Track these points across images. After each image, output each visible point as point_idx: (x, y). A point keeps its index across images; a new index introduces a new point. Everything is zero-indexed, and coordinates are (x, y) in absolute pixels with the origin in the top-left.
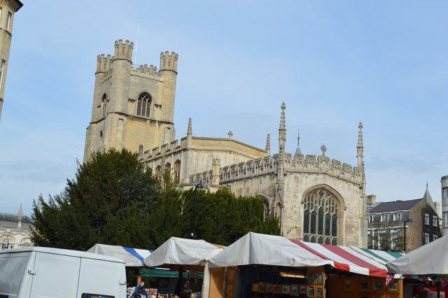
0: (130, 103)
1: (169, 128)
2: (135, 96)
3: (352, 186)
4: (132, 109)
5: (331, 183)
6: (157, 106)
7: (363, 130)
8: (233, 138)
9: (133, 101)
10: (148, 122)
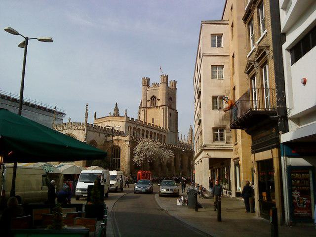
2: (149, 98)
3: (81, 131)
4: (149, 104)
6: (158, 100)
9: (149, 101)
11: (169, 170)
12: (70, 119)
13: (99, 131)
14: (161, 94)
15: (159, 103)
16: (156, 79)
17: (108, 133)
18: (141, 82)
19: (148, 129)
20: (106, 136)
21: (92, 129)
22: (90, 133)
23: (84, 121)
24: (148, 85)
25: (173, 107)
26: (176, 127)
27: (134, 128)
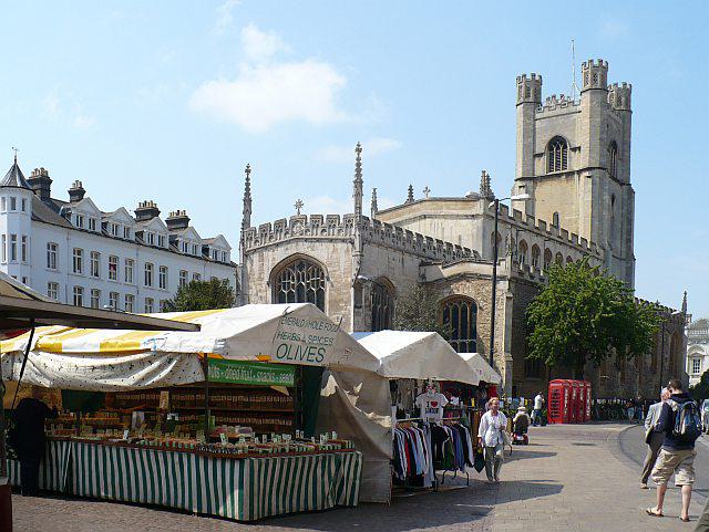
0: (537, 159)
2: (541, 147)
4: (541, 167)
5: (304, 248)
6: (574, 150)
8: (431, 195)
9: (540, 155)
12: (299, 205)
13: (400, 245)
14: (582, 133)
15: (577, 161)
16: (565, 82)
17: (429, 253)
18: (512, 93)
19: (549, 245)
20: (422, 264)
21: (377, 238)
22: (372, 250)
23: (351, 210)
24: (538, 102)
26: (629, 241)
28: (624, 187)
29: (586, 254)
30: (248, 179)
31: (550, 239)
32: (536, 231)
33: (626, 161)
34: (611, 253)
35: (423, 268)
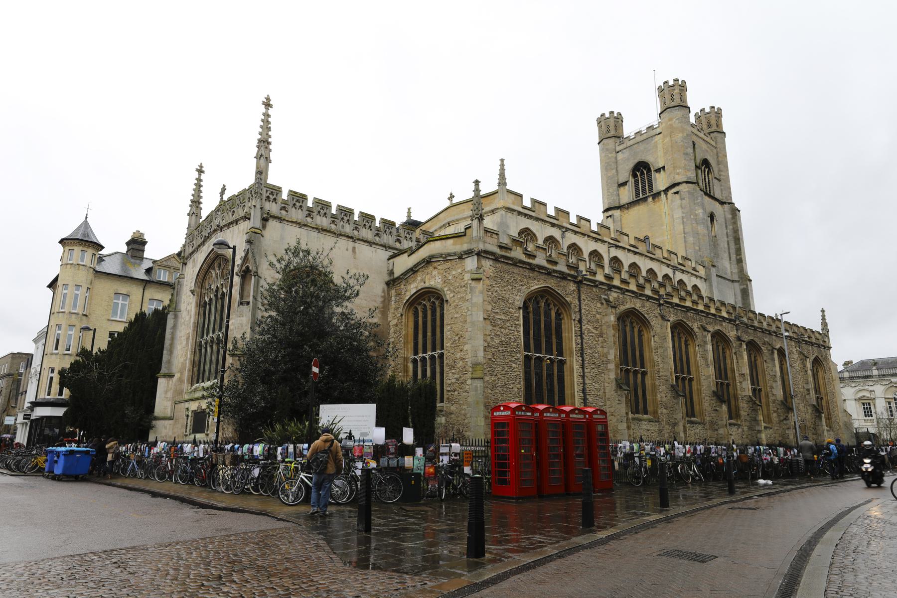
0: (622, 188)
1: (677, 193)
2: (625, 174)
4: (627, 194)
6: (658, 170)
7: (271, 111)
8: (455, 201)
9: (624, 184)
10: (650, 199)
11: (734, 414)
13: (348, 229)
15: (660, 182)
18: (594, 134)
19: (614, 252)
21: (297, 215)
25: (717, 195)
26: (740, 261)
27: (550, 239)
28: (726, 206)
29: (675, 269)
30: (199, 180)
31: (617, 247)
32: (592, 234)
33: (724, 180)
34: (714, 271)
35: (391, 261)
